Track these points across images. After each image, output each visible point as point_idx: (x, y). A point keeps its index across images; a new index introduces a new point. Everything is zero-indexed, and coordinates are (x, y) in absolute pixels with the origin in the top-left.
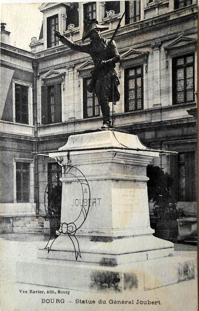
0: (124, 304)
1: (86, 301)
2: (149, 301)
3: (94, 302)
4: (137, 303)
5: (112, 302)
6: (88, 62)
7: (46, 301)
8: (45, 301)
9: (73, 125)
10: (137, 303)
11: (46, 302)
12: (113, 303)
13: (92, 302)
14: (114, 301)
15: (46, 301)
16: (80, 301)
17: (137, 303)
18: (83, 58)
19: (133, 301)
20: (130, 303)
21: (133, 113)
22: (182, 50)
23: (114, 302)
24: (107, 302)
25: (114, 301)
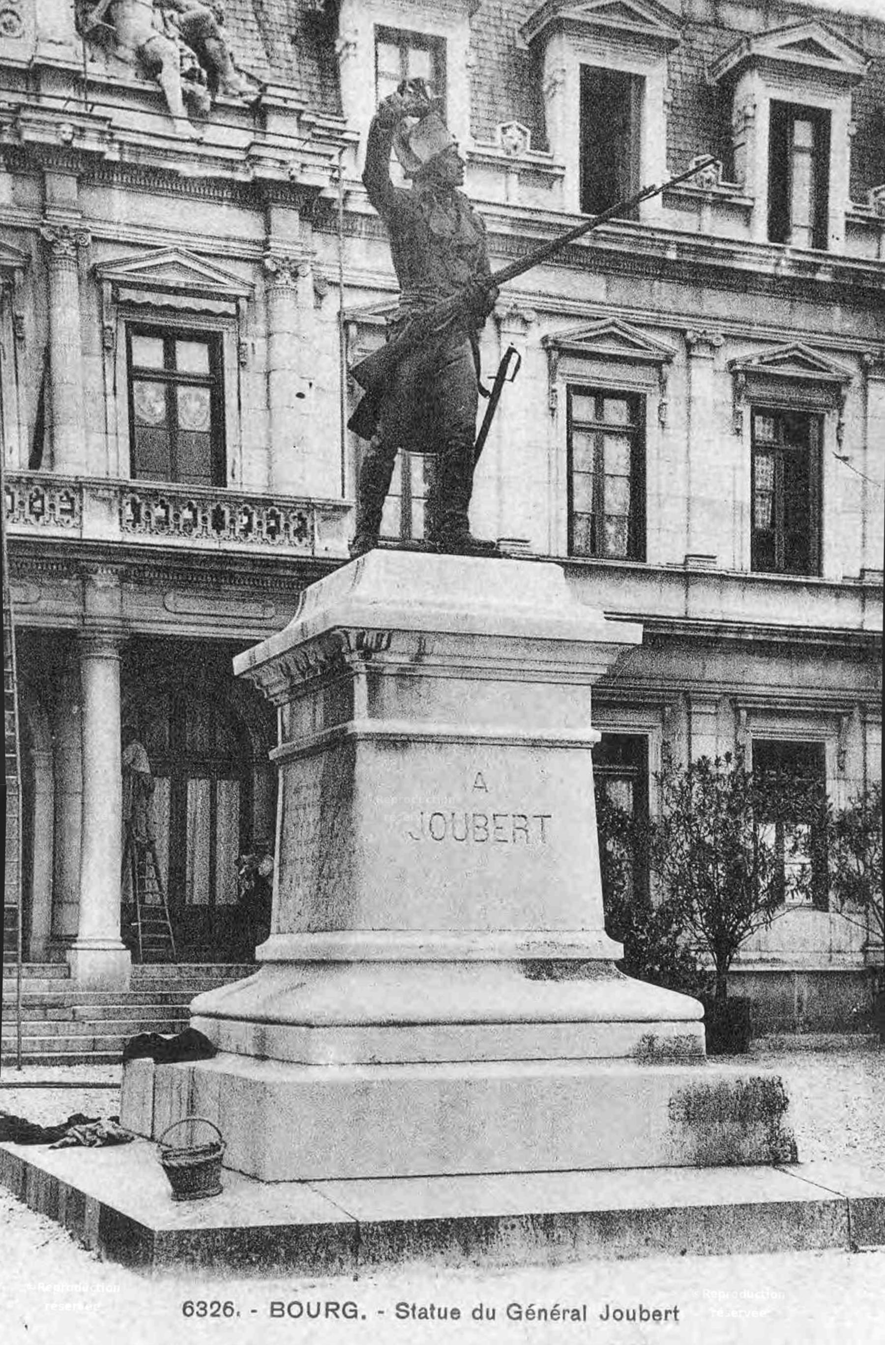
0: (290, 1301)
1: (432, 1308)
2: (644, 1308)
3: (456, 1313)
4: (601, 1317)
5: (516, 1313)
6: (607, 326)
7: (285, 1309)
8: (281, 1310)
9: (857, 601)
10: (605, 1316)
11: (286, 1314)
12: (520, 1318)
13: (449, 1315)
14: (524, 1310)
15: (285, 1309)
16: (414, 1308)
17: (601, 1317)
18: (693, 316)
19: (585, 1307)
20: (576, 1315)
21: (628, 569)
22: (839, 362)
23: (527, 1314)
24: (501, 1311)
25: (524, 1310)
